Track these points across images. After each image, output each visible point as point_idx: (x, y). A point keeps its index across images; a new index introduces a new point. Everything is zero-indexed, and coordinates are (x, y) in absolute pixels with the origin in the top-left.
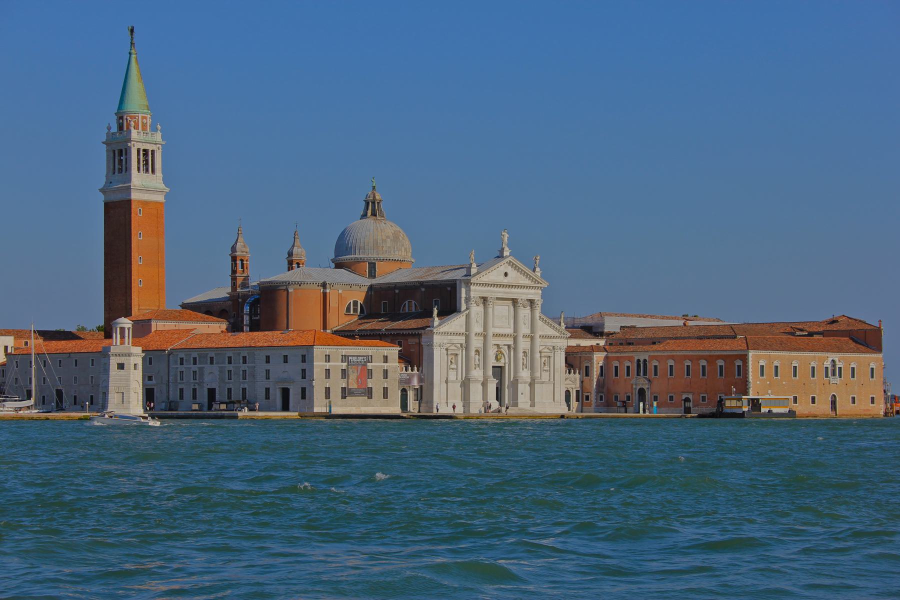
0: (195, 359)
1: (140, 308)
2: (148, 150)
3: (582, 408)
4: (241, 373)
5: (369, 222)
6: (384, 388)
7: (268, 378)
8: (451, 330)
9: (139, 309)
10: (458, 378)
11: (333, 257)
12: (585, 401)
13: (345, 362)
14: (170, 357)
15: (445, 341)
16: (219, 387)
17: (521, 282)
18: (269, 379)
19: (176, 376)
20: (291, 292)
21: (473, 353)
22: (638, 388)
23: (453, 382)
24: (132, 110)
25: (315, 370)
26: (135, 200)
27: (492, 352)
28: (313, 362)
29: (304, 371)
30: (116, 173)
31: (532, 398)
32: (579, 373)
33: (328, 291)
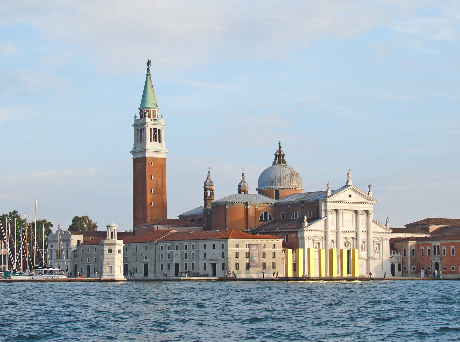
0: (169, 247)
1: (152, 218)
2: (156, 129)
3: (402, 274)
4: (192, 255)
5: (277, 166)
6: (273, 263)
7: (205, 257)
8: (315, 229)
9: (151, 219)
11: (257, 187)
14: (157, 246)
15: (312, 235)
19: (159, 256)
20: (227, 208)
21: (329, 242)
22: (435, 262)
24: (147, 107)
25: (229, 253)
26: (148, 157)
27: (342, 242)
29: (223, 253)
30: (139, 142)
33: (249, 207)
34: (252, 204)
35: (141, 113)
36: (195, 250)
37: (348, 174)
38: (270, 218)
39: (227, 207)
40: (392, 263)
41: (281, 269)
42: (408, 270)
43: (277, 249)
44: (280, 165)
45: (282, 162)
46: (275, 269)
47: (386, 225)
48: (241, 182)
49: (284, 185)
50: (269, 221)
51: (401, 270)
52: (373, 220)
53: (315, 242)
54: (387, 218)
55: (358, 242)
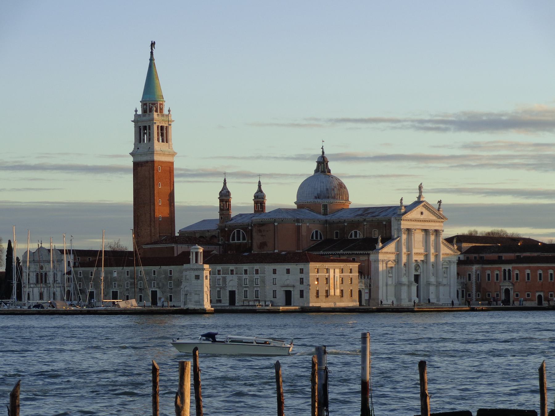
2: (164, 126)
4: (254, 280)
8: (389, 251)
9: (160, 236)
11: (296, 200)
12: (468, 297)
15: (386, 258)
16: (238, 290)
17: (431, 218)
22: (505, 288)
26: (156, 161)
28: (308, 273)
34: (303, 221)
35: (145, 106)
36: (259, 275)
38: (321, 238)
39: (276, 224)
42: (472, 297)
43: (354, 274)
44: (324, 173)
50: (320, 240)
51: (465, 297)
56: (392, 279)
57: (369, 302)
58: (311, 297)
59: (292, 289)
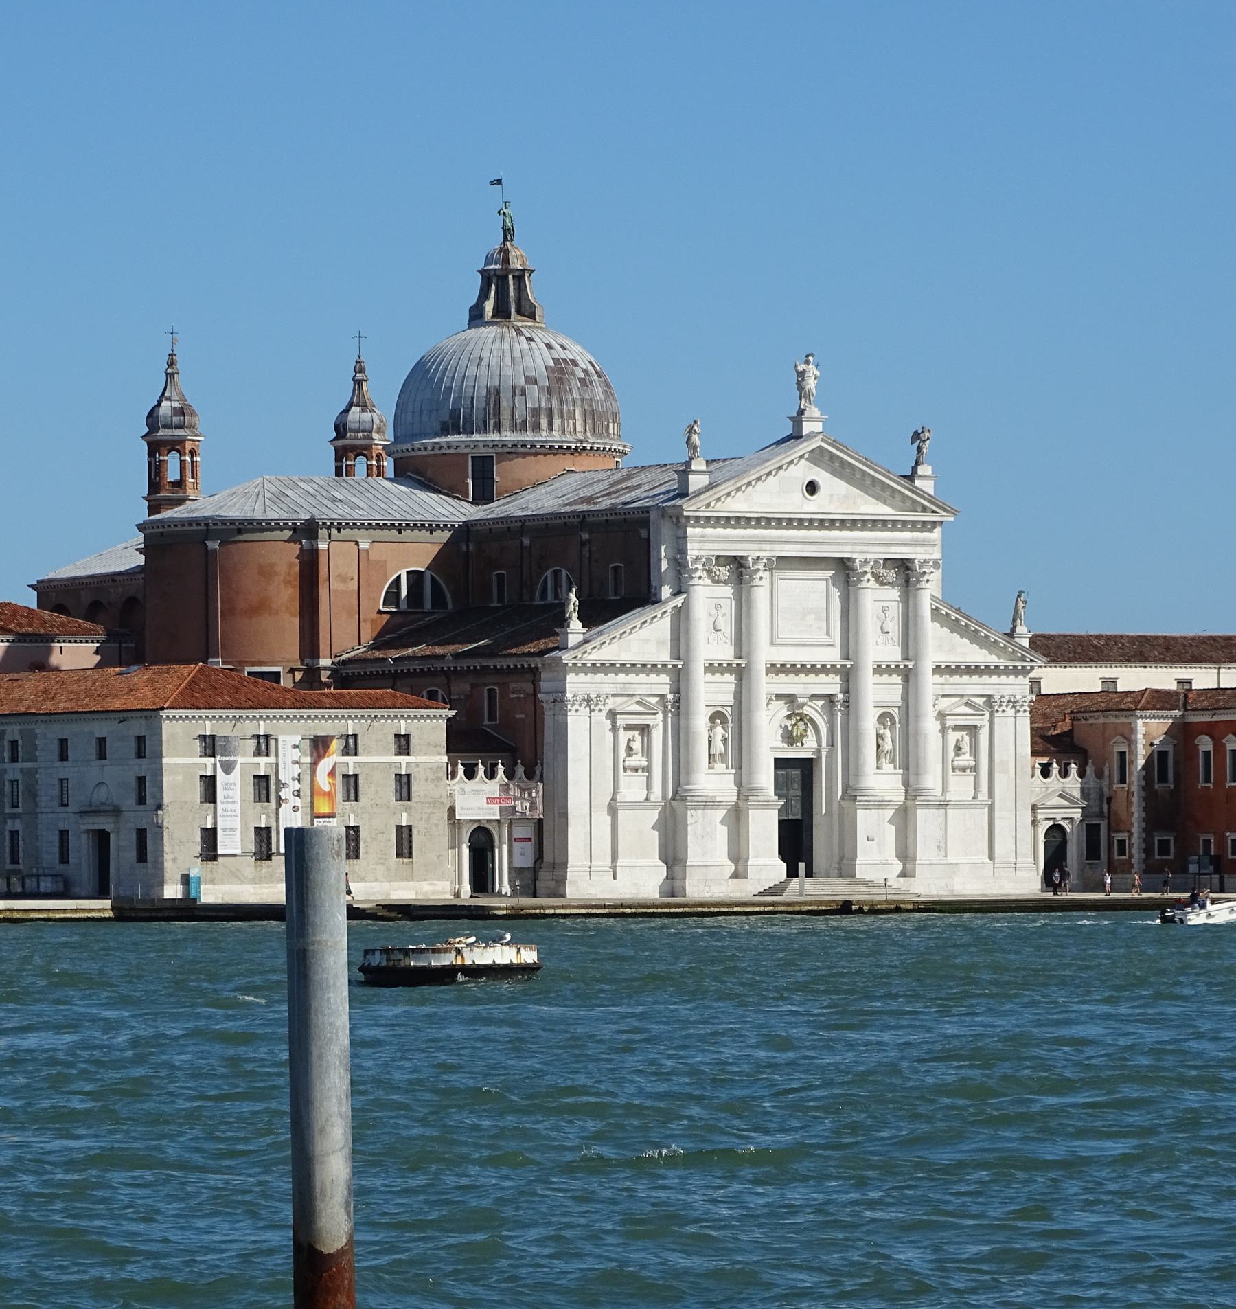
4: (7, 788)
6: (399, 828)
10: (652, 798)
13: (267, 755)
18: (67, 805)
23: (633, 806)
25: (167, 780)
28: (159, 756)
29: (141, 781)
31: (906, 853)
32: (1081, 774)
33: (322, 545)
37: (803, 380)
39: (214, 545)
40: (1051, 823)
41: (439, 857)
42: (1131, 857)
45: (519, 312)
46: (410, 856)
47: (1011, 635)
48: (351, 405)
49: (514, 428)
50: (429, 613)
52: (937, 609)
53: (621, 721)
54: (1019, 596)
55: (857, 719)
56: (649, 779)
57: (535, 879)
58: (174, 860)
59: (112, 826)
